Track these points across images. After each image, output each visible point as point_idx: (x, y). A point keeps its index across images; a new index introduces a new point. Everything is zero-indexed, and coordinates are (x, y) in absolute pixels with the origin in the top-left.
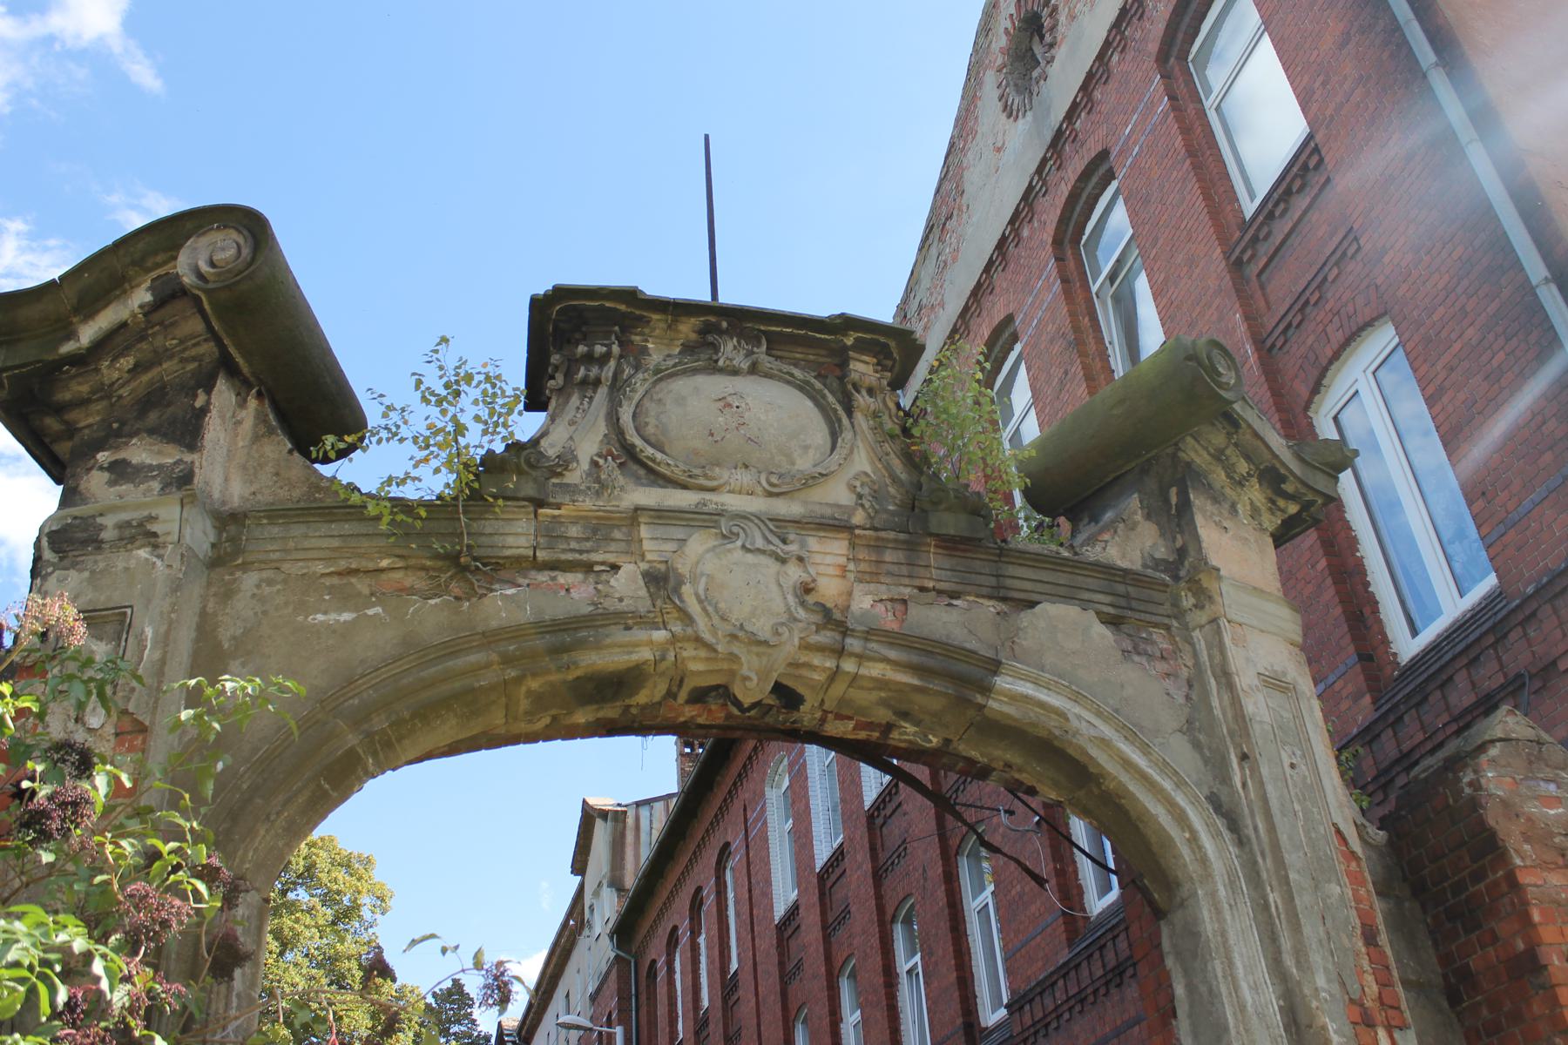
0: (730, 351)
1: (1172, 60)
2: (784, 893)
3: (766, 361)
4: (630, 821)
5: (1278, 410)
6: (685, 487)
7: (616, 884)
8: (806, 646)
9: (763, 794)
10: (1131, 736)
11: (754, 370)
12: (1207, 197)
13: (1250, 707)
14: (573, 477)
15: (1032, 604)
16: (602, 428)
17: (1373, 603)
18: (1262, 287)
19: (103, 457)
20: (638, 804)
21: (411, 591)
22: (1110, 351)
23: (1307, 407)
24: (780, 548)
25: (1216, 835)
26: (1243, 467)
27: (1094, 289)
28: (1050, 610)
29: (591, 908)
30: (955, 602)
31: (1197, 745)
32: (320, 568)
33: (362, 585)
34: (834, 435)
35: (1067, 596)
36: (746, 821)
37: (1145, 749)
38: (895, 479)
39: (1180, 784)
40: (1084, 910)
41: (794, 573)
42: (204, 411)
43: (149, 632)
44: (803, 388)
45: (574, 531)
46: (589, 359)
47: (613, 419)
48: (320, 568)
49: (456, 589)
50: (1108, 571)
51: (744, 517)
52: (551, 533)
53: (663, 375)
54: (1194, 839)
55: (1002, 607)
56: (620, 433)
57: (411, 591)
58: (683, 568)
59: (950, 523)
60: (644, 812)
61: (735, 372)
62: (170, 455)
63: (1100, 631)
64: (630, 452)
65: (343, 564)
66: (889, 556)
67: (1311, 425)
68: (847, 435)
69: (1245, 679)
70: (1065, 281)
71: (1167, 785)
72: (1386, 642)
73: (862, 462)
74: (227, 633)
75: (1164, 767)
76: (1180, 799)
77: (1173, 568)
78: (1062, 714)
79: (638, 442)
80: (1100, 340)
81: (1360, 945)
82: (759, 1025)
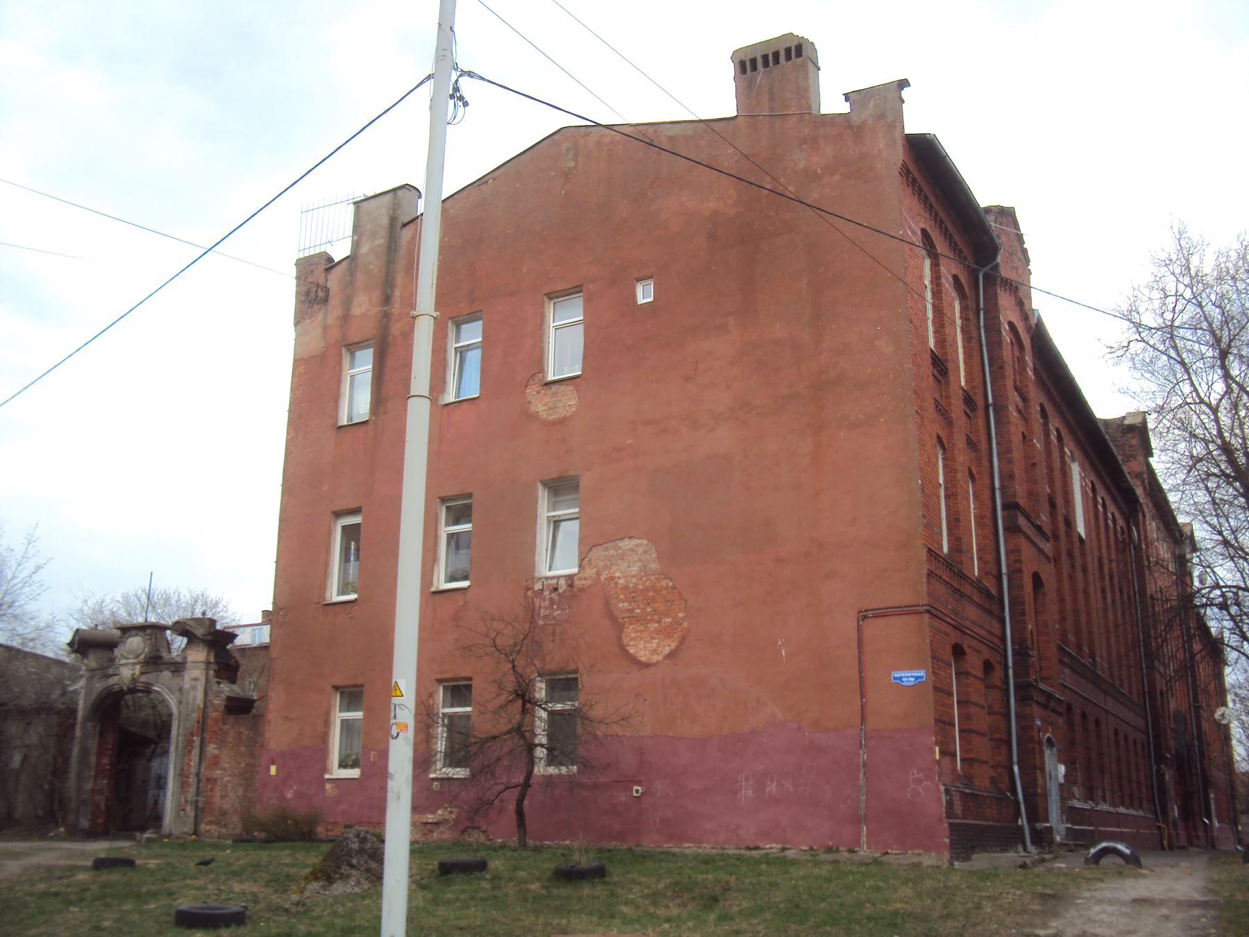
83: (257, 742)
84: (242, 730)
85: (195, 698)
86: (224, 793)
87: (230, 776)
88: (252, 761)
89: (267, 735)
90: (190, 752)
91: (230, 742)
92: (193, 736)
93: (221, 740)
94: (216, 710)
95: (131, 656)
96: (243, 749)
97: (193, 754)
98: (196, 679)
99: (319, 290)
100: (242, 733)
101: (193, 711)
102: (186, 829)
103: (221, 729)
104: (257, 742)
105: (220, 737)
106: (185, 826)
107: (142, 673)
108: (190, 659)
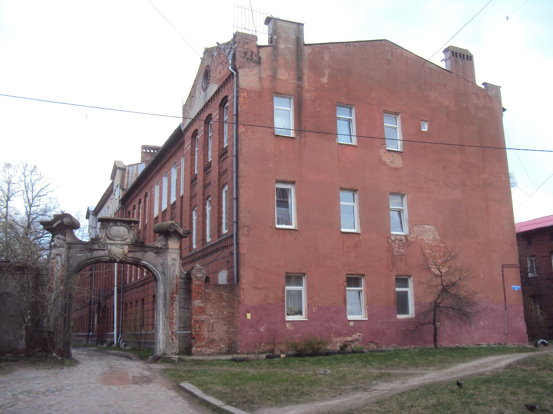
0: (119, 224)
1: (222, 107)
2: (156, 213)
3: (123, 224)
4: (127, 171)
5: (218, 187)
6: (113, 240)
7: (122, 188)
8: (123, 257)
9: (154, 186)
10: (154, 267)
11: (121, 226)
12: (219, 141)
13: (169, 263)
14: (102, 240)
15: (147, 252)
16: (105, 233)
17: (222, 224)
18: (222, 163)
19: (56, 236)
20: (129, 166)
21: (87, 252)
22: (209, 151)
23: (222, 188)
24: (121, 247)
25: (161, 276)
26: (176, 233)
27: (209, 136)
28: (150, 253)
29: (115, 190)
30: (139, 252)
31: (162, 267)
32: (78, 250)
33: (82, 251)
34: (129, 232)
35: (151, 251)
36: (151, 190)
37: (156, 268)
38: (135, 238)
39: (159, 271)
40: (192, 247)
41: (123, 250)
42: (66, 232)
43: (63, 257)
44: (126, 227)
45: (102, 246)
46: (104, 225)
47: (106, 232)
48: (78, 250)
49: (91, 252)
50: (157, 248)
51: (118, 244)
52: (99, 246)
53: (111, 227)
54: (159, 277)
55: (144, 253)
56: (107, 234)
57: (87, 252)
58: (112, 249)
59: (139, 244)
60: (131, 168)
61: (119, 226)
62: (63, 237)
63: (154, 255)
64: (108, 236)
65: (80, 249)
66: (133, 248)
67: (222, 192)
68: (130, 233)
69: (169, 259)
70: (205, 132)
71: (157, 271)
72: (222, 230)
73: (131, 236)
74: (70, 256)
75: (157, 270)
76: (158, 273)
77: (165, 246)
78: (147, 265)
79: (108, 235)
80: (208, 148)
81: (175, 287)
82: (149, 239)
83: (235, 300)
84: (223, 293)
85: (174, 271)
86: (211, 329)
87: (215, 319)
88: (232, 310)
89: (242, 297)
90: (173, 304)
91: (213, 299)
92: (174, 294)
93: (205, 298)
94: (199, 280)
95: (118, 239)
96: (224, 304)
97: (174, 305)
98: (174, 259)
99: (253, 55)
100: (223, 294)
101: (173, 279)
102: (174, 351)
103: (204, 292)
104: (235, 300)
105: (204, 296)
106: (174, 349)
107: (129, 251)
108: (170, 247)
